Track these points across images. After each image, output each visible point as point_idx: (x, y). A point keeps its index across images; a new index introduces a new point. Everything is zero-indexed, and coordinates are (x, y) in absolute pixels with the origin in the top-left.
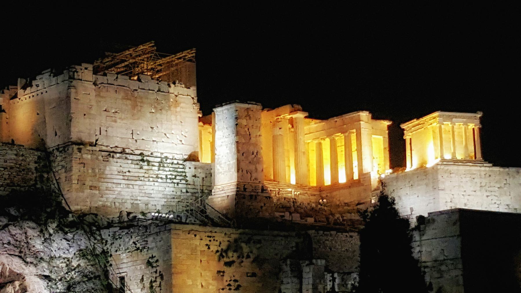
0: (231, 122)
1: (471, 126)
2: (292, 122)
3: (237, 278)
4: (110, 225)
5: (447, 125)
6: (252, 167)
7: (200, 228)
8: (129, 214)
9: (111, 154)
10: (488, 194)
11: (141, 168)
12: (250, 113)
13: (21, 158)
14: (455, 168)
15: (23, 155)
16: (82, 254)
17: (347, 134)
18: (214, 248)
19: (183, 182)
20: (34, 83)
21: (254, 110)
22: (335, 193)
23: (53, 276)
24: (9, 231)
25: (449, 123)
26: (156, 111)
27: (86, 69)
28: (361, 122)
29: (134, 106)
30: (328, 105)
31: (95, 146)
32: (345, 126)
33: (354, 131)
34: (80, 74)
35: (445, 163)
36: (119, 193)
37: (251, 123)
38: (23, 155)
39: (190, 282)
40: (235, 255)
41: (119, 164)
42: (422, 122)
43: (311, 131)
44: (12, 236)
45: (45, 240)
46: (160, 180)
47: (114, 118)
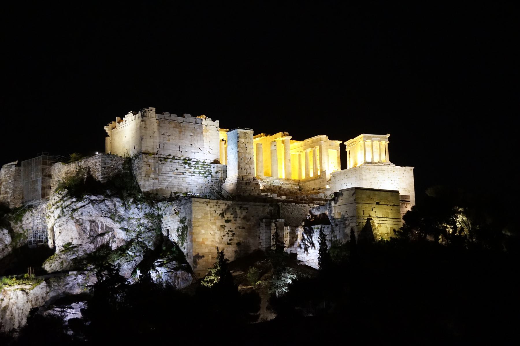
0: (235, 140)
2: (283, 142)
3: (233, 229)
4: (163, 200)
5: (369, 142)
7: (211, 201)
8: (175, 193)
9: (166, 159)
10: (392, 182)
12: (247, 135)
13: (114, 162)
14: (373, 167)
15: (115, 161)
16: (147, 216)
17: (314, 149)
18: (219, 212)
19: (210, 176)
20: (124, 119)
22: (306, 183)
23: (130, 229)
24: (105, 204)
26: (194, 135)
27: (151, 110)
29: (180, 132)
30: (301, 131)
34: (147, 113)
36: (171, 182)
37: (247, 140)
38: (115, 161)
39: (203, 231)
40: (233, 216)
41: (171, 165)
44: (107, 206)
45: (126, 209)
46: (195, 175)
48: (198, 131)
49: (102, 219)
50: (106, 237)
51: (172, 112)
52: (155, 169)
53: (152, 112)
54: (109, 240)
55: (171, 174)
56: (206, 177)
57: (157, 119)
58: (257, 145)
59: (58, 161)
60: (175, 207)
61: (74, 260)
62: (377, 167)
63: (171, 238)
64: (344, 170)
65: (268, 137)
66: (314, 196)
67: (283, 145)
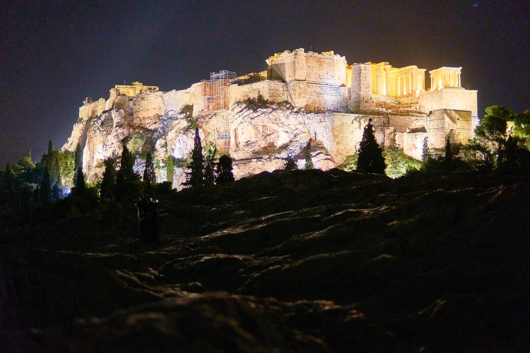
2: (385, 69)
4: (310, 112)
6: (367, 90)
8: (318, 108)
29: (320, 65)
36: (314, 100)
37: (366, 72)
48: (332, 65)
49: (271, 125)
50: (272, 136)
53: (301, 51)
54: (275, 138)
55: (314, 94)
59: (235, 83)
61: (254, 152)
62: (452, 90)
63: (317, 138)
66: (409, 109)
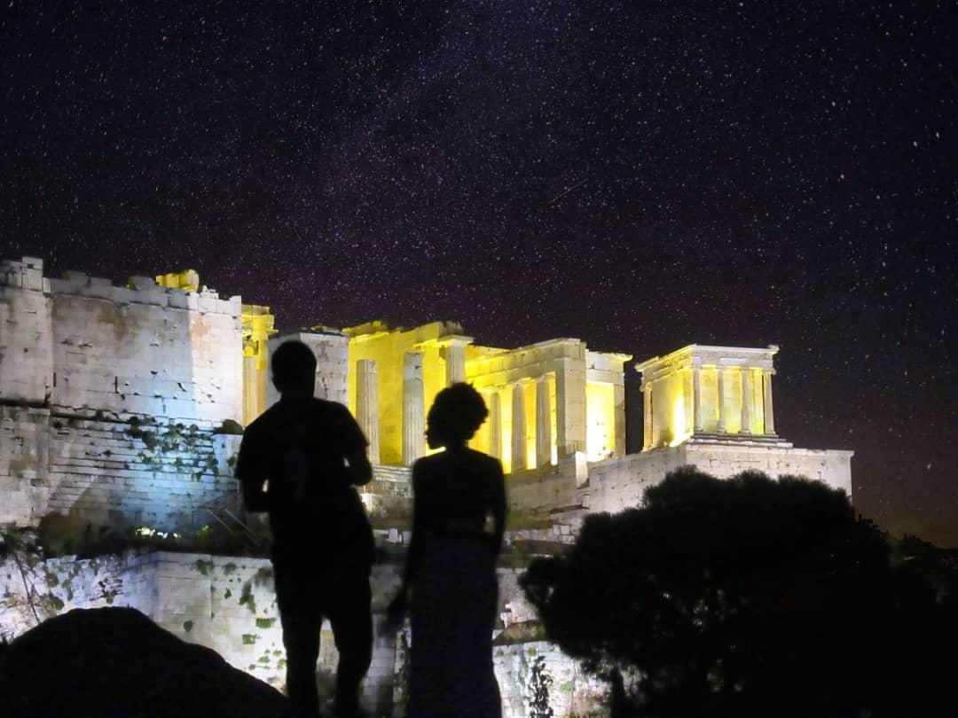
1: (758, 372)
5: (710, 371)
11: (131, 448)
12: (327, 349)
14: (720, 449)
17: (541, 380)
21: (336, 345)
25: (714, 366)
27: (30, 266)
28: (566, 359)
29: (120, 334)
31: (45, 404)
32: (538, 364)
33: (553, 373)
34: (19, 277)
35: (701, 441)
41: (88, 440)
42: (668, 363)
43: (481, 372)
47: (81, 356)
51: (95, 271)
52: (39, 449)
55: (88, 467)
56: (199, 475)
57: (46, 295)
58: (360, 364)
60: (100, 577)
64: (632, 457)
65: (398, 335)
67: (442, 362)
